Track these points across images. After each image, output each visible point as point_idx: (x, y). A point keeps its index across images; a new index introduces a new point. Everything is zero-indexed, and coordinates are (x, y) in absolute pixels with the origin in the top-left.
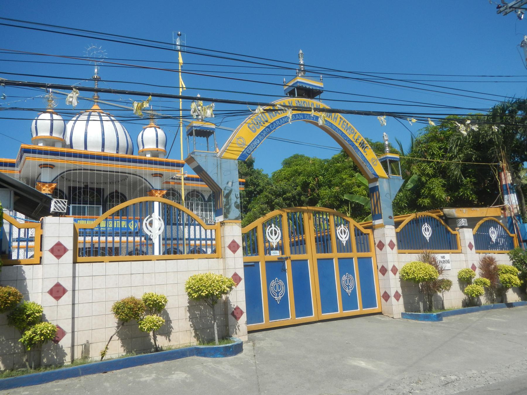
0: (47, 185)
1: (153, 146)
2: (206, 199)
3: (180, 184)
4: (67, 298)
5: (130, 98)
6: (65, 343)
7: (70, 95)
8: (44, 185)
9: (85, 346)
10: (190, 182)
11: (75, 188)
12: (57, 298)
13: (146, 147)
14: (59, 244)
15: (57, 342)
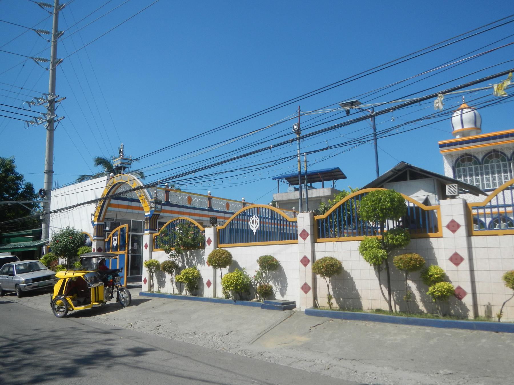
4: (465, 265)
5: (489, 83)
6: (467, 300)
7: (437, 101)
9: (487, 306)
12: (457, 264)
14: (453, 221)
15: (460, 299)
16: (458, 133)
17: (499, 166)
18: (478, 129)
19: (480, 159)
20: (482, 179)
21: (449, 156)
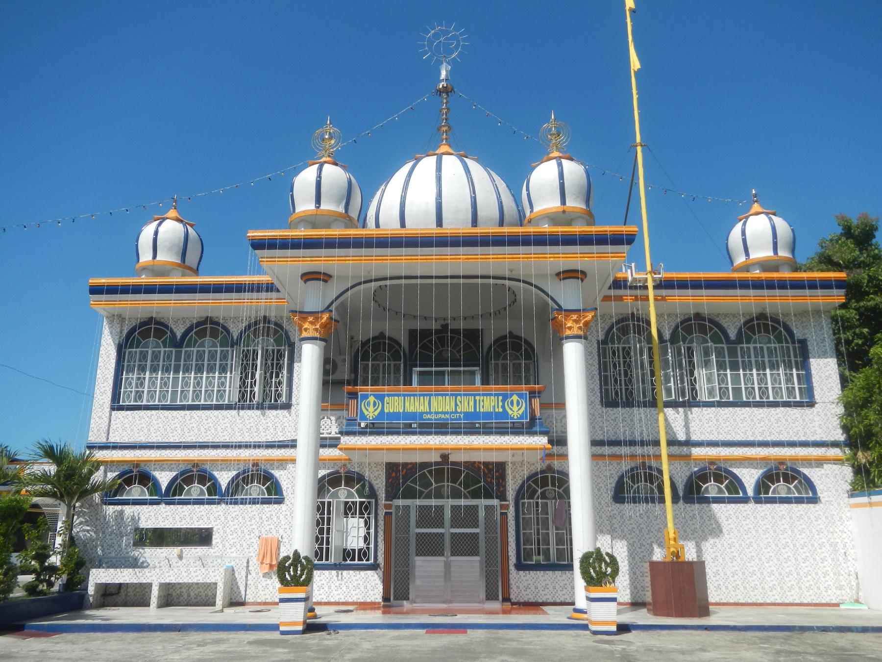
0: (311, 319)
1: (552, 203)
2: (732, 335)
3: (647, 298)
8: (304, 319)
10: (676, 292)
11: (426, 333)
13: (536, 209)
16: (145, 269)
17: (212, 356)
18: (190, 268)
19: (179, 335)
20: (176, 380)
21: (117, 318)
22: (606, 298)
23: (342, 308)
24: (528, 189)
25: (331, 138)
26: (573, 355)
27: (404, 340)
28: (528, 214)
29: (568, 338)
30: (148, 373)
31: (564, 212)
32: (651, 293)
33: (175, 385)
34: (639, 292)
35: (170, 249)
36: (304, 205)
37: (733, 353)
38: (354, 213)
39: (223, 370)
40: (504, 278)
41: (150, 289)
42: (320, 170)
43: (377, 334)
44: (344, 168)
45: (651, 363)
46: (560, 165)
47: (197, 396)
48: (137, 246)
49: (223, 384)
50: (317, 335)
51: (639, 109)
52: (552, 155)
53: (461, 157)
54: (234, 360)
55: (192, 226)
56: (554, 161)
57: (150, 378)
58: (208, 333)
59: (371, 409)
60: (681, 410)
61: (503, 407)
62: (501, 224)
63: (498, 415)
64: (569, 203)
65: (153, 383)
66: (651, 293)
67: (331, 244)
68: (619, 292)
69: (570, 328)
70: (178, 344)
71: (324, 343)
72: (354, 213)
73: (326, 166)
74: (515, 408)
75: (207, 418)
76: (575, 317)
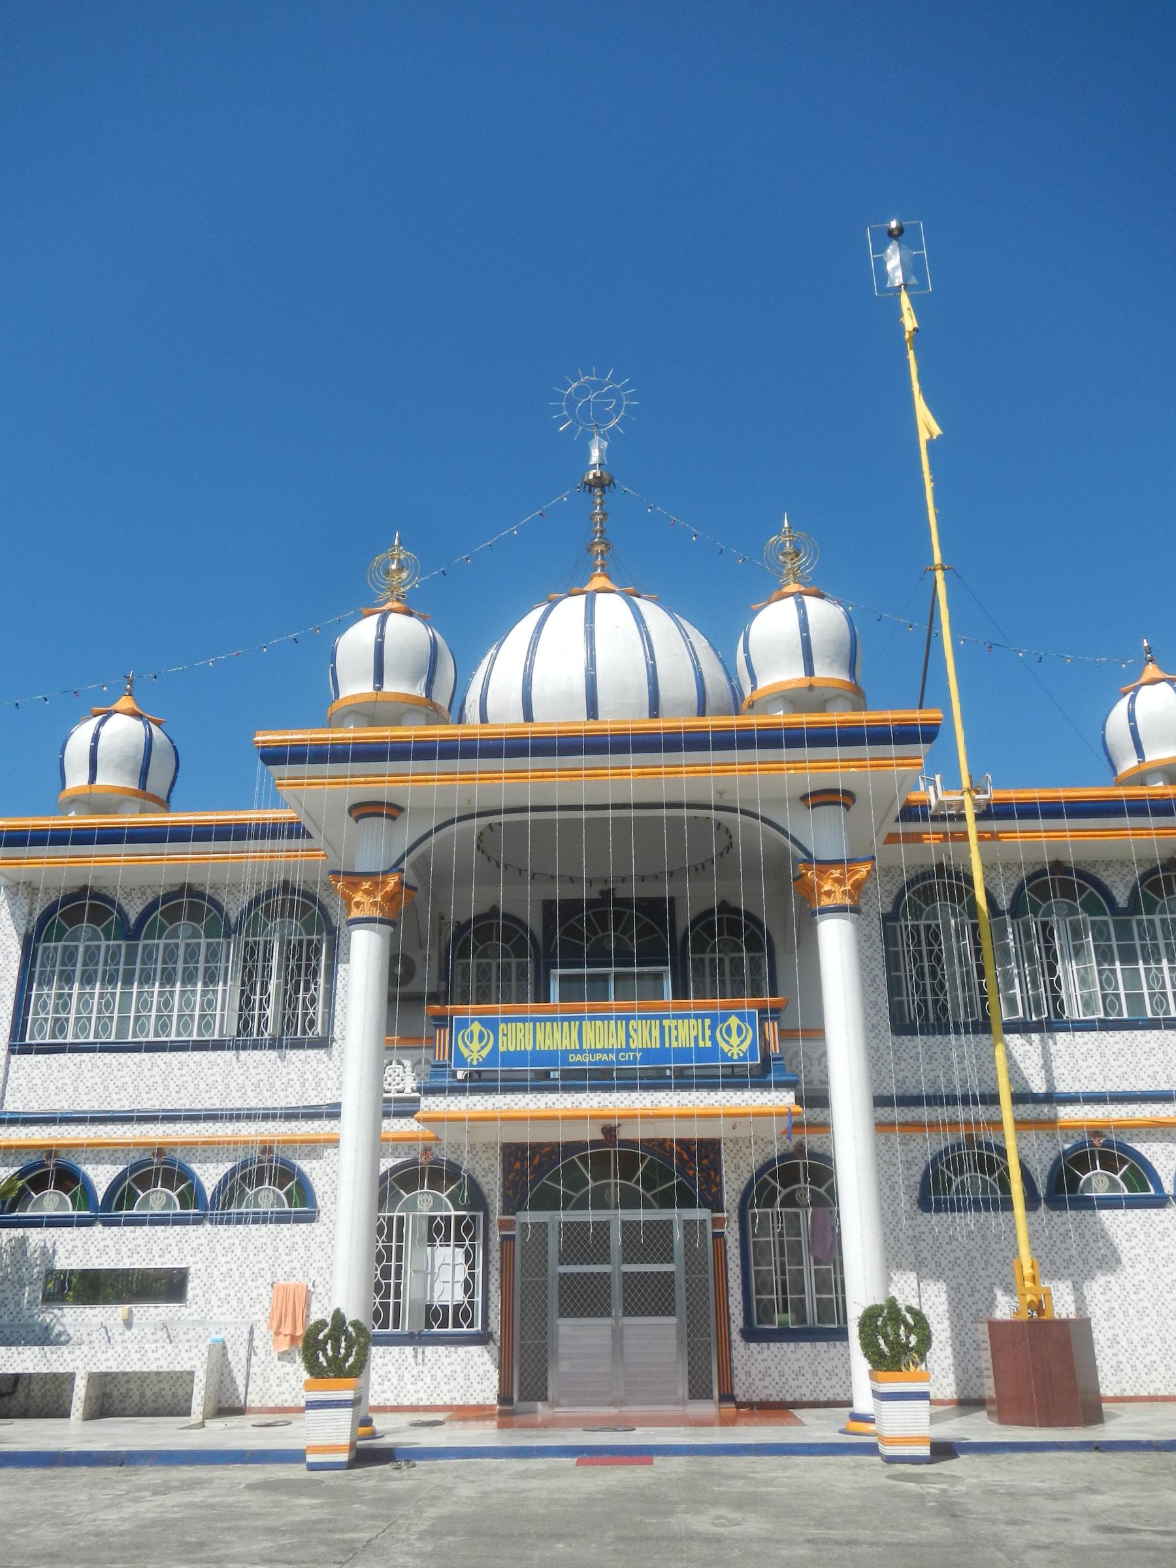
0: (366, 885)
1: (791, 674)
2: (1122, 900)
3: (965, 837)
8: (355, 886)
10: (1017, 824)
11: (571, 907)
13: (762, 683)
16: (76, 801)
17: (192, 953)
18: (154, 798)
19: (133, 917)
20: (126, 996)
21: (21, 889)
22: (892, 838)
23: (422, 865)
24: (746, 649)
25: (400, 569)
26: (837, 944)
27: (532, 918)
28: (748, 693)
29: (825, 911)
30: (76, 986)
31: (811, 687)
32: (971, 826)
33: (125, 1007)
34: (948, 826)
35: (119, 765)
36: (355, 685)
37: (1124, 931)
38: (442, 698)
39: (211, 978)
40: (707, 807)
41: (83, 837)
42: (382, 623)
43: (485, 909)
44: (424, 619)
45: (978, 952)
46: (801, 606)
47: (163, 1025)
48: (62, 760)
49: (210, 1004)
50: (377, 914)
51: (936, 506)
52: (786, 590)
53: (628, 596)
54: (232, 961)
55: (158, 724)
56: (791, 599)
57: (81, 995)
58: (185, 911)
59: (475, 1045)
60: (1035, 1037)
61: (713, 1038)
62: (702, 711)
63: (702, 1053)
64: (821, 672)
65: (86, 1004)
66: (971, 826)
67: (400, 752)
68: (913, 827)
69: (829, 894)
70: (130, 932)
71: (388, 929)
72: (442, 698)
73: (394, 620)
74: (735, 1040)
75: (146, 1065)
76: (836, 873)
